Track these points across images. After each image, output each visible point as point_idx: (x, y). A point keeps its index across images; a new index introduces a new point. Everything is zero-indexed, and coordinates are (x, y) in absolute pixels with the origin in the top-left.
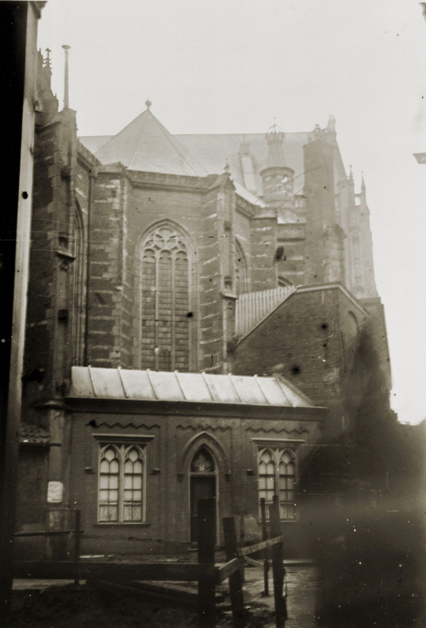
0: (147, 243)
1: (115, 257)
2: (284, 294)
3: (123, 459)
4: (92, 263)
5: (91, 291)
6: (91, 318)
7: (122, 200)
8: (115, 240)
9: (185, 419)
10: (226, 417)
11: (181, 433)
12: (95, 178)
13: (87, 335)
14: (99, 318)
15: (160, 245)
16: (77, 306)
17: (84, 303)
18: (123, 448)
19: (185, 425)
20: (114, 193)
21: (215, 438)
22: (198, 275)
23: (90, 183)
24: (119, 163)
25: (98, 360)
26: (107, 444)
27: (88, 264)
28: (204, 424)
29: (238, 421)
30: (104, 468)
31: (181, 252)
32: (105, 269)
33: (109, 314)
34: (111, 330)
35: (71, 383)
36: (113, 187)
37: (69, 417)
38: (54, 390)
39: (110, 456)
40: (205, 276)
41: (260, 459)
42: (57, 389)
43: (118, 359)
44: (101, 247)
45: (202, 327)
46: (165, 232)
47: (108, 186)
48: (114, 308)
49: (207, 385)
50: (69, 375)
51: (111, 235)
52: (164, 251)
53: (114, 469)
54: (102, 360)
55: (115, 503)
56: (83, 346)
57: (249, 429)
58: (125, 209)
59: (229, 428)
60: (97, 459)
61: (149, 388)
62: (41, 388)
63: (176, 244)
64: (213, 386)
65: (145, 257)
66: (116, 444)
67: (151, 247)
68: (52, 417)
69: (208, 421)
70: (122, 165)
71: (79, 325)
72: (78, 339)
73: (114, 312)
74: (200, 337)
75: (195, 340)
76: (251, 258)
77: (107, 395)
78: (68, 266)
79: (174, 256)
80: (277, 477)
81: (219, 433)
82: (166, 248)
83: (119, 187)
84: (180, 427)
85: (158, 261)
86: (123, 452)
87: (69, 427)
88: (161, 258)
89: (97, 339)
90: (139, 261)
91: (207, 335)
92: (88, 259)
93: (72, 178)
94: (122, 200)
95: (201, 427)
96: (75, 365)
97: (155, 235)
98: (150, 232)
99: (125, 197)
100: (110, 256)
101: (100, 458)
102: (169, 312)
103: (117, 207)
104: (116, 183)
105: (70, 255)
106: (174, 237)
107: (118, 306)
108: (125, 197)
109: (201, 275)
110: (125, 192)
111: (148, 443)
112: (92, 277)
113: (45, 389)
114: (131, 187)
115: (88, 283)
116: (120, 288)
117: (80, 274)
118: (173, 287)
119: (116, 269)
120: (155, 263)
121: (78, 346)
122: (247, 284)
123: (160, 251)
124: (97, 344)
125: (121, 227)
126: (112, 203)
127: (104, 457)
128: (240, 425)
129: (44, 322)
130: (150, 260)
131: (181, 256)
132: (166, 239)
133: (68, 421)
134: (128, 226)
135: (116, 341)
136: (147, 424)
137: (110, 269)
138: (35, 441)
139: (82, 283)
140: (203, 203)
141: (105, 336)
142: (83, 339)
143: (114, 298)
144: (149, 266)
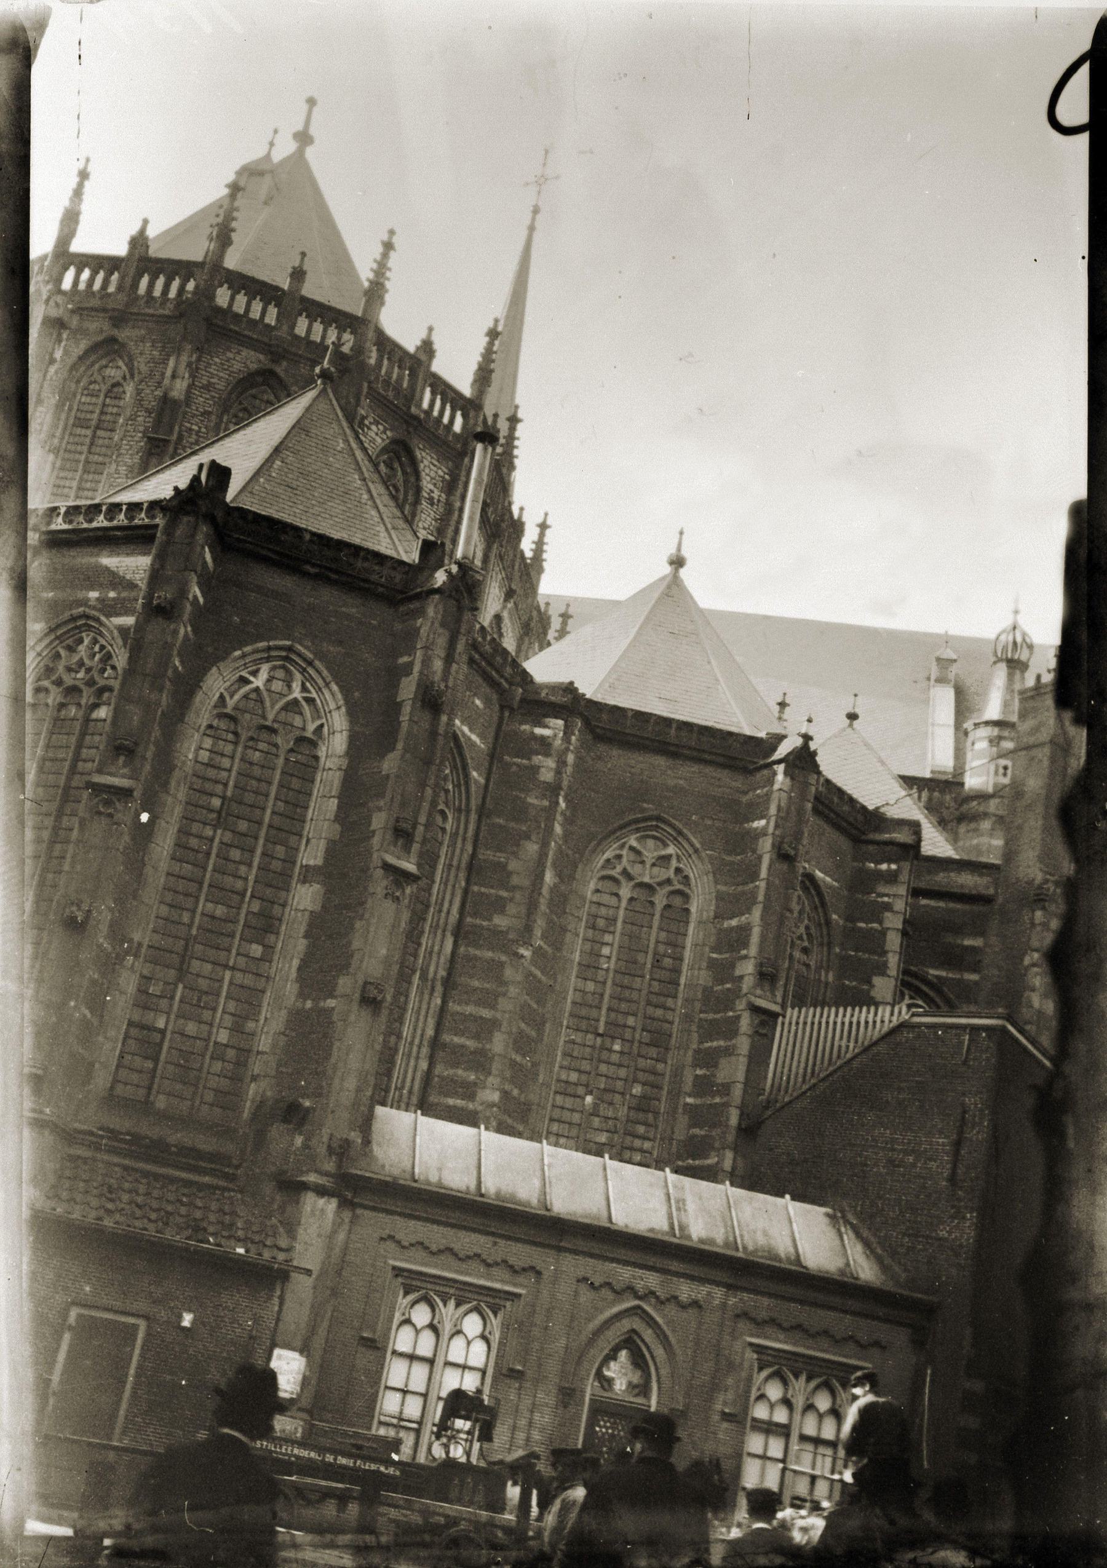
0: (608, 861)
1: (526, 883)
2: (882, 1021)
3: (447, 1328)
4: (476, 888)
5: (462, 949)
6: (453, 1007)
7: (562, 763)
8: (532, 848)
9: (600, 1265)
10: (692, 1278)
11: (586, 1296)
12: (512, 710)
13: (435, 1043)
14: (469, 1009)
15: (635, 870)
16: (424, 977)
17: (442, 973)
18: (452, 1304)
20: (544, 745)
21: (659, 1320)
22: (707, 949)
23: (501, 719)
24: (572, 683)
25: (451, 1101)
26: (417, 1289)
27: (466, 892)
28: (639, 1286)
29: (718, 1293)
30: (403, 1340)
31: (679, 892)
32: (499, 906)
33: (493, 1007)
35: (367, 1142)
36: (546, 732)
37: (347, 1215)
38: (322, 1150)
39: (421, 1315)
40: (720, 953)
41: (759, 1389)
42: (330, 1149)
43: (493, 1105)
44: (501, 857)
45: (695, 1065)
46: (650, 843)
47: (538, 731)
48: (504, 995)
49: (668, 1195)
50: (366, 1124)
51: (528, 837)
52: (641, 885)
53: (426, 1345)
55: (414, 1426)
56: (424, 1065)
57: (743, 1315)
58: (565, 784)
59: (695, 1304)
60: (390, 1319)
61: (537, 1183)
62: (299, 1141)
63: (671, 873)
64: (681, 1204)
65: (597, 891)
66: (438, 1293)
67: (616, 872)
68: (308, 1208)
69: (651, 1280)
70: (576, 689)
71: (422, 1018)
72: (415, 1049)
73: (504, 1004)
74: (688, 1086)
75: (675, 1094)
76: (845, 927)
77: (440, 1185)
79: (660, 900)
80: (794, 1437)
81: (671, 1310)
82: (647, 879)
83: (561, 734)
85: (624, 904)
86: (448, 1312)
87: (341, 1236)
88: (631, 899)
89: (458, 1056)
90: (583, 898)
91: (703, 1086)
92: (468, 881)
93: (445, 707)
94: (562, 763)
95: (631, 1289)
96: (383, 1104)
97: (627, 846)
98: (618, 839)
99: (570, 758)
100: (515, 880)
101: (398, 1317)
102: (631, 1021)
103: (547, 775)
104: (552, 729)
105: (411, 867)
106: (668, 858)
107: (513, 991)
108: (570, 758)
109: (714, 949)
110: (572, 748)
111: (508, 1304)
112: (469, 919)
113: (306, 1146)
114: (590, 737)
115: (458, 932)
116: (526, 953)
118: (649, 966)
120: (618, 908)
121: (412, 1063)
122: (827, 984)
123: (632, 883)
124: (456, 1065)
125: (551, 819)
126: (535, 769)
127: (407, 1316)
128: (724, 1305)
129: (331, 1003)
130: (606, 899)
131: (677, 901)
132: (650, 855)
133: (340, 1224)
134: (569, 821)
135: (496, 1067)
136: (512, 1260)
137: (511, 909)
138: (260, 1254)
139: (444, 931)
140: (746, 793)
142: (425, 1050)
143: (508, 972)
144: (603, 911)
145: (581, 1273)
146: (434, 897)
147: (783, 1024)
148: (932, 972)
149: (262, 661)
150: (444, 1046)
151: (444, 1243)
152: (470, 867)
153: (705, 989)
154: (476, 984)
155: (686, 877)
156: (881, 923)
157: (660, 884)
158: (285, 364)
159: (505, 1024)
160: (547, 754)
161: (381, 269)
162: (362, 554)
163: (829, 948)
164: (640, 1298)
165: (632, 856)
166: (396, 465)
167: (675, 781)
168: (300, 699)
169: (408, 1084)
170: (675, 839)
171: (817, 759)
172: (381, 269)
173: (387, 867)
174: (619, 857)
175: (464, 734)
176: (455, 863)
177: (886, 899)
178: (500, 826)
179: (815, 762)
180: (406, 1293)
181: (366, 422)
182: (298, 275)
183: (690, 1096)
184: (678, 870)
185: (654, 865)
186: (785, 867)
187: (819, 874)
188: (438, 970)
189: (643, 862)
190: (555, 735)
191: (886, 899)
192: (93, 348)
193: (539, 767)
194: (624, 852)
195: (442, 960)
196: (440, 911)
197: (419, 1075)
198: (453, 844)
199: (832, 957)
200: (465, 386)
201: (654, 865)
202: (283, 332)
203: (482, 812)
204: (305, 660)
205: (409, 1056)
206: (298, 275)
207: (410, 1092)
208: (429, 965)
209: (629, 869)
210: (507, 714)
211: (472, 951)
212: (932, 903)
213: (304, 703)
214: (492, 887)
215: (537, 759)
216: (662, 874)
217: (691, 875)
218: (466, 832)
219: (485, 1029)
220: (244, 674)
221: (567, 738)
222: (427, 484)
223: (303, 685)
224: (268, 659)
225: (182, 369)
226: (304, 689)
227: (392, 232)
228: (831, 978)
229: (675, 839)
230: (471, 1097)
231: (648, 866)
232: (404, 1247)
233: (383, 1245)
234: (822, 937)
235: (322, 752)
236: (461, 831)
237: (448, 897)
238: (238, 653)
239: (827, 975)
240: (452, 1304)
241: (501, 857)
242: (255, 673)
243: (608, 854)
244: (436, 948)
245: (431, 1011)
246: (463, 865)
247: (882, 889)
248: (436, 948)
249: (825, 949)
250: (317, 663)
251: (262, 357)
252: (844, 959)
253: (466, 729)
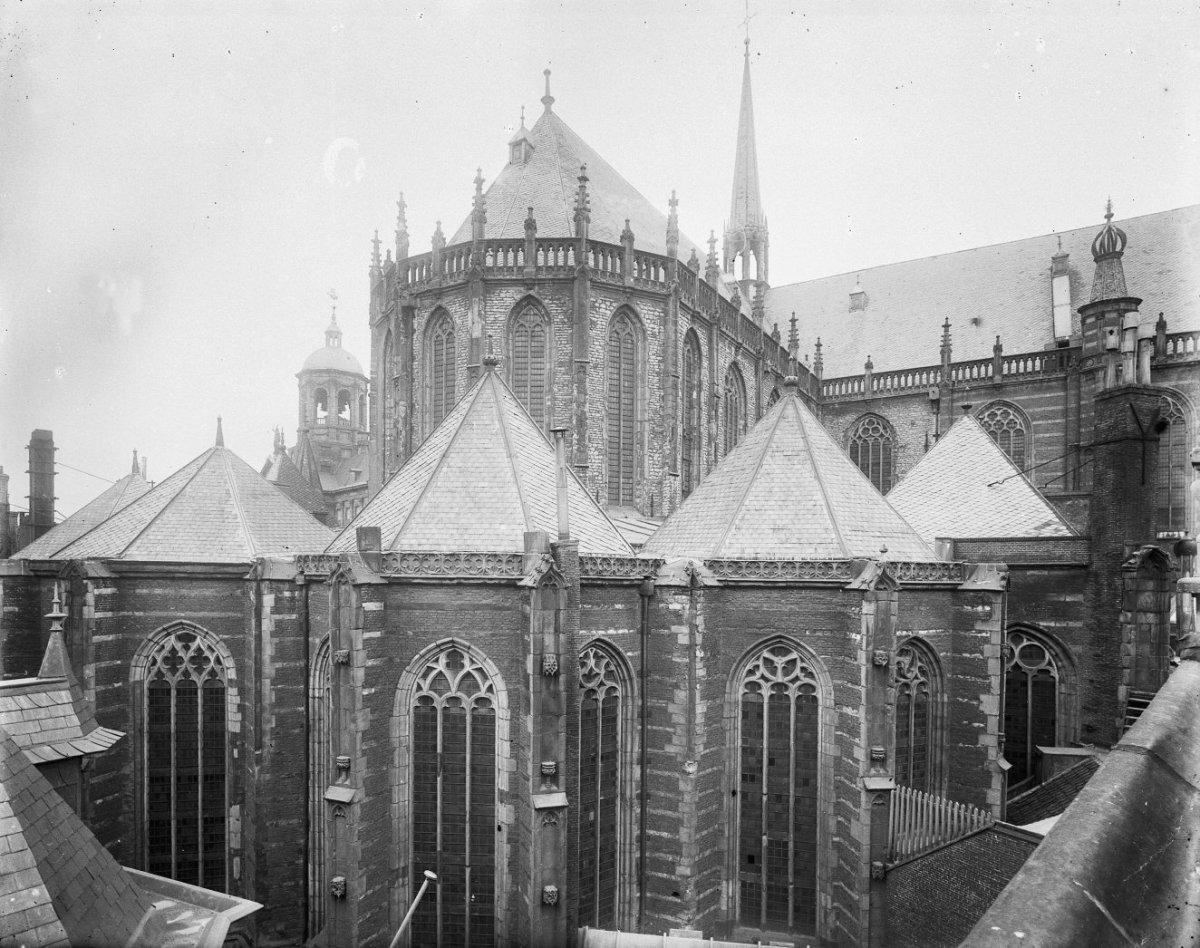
1: (682, 720)
5: (648, 771)
7: (693, 627)
8: (681, 695)
13: (642, 839)
23: (643, 602)
25: (660, 875)
33: (675, 809)
51: (677, 686)
72: (628, 847)
73: (682, 807)
78: (557, 818)
85: (766, 700)
92: (642, 725)
94: (693, 627)
97: (762, 658)
99: (700, 621)
106: (794, 661)
107: (687, 798)
117: (629, 750)
119: (684, 740)
122: (943, 703)
123: (770, 684)
124: (658, 850)
137: (675, 740)
139: (632, 764)
141: (668, 841)
143: (682, 786)
146: (619, 744)
147: (895, 796)
148: (1042, 624)
149: (438, 653)
150: (649, 837)
152: (642, 715)
153: (836, 758)
154: (662, 794)
156: (982, 653)
158: (536, 288)
159: (685, 820)
160: (680, 623)
163: (942, 676)
166: (627, 320)
167: (789, 607)
169: (627, 871)
175: (610, 636)
176: (629, 715)
177: (984, 634)
178: (659, 682)
181: (597, 305)
182: (530, 225)
183: (836, 836)
187: (922, 633)
188: (632, 791)
190: (683, 608)
191: (984, 634)
192: (433, 314)
193: (677, 634)
194: (760, 662)
196: (626, 752)
197: (634, 864)
198: (625, 705)
199: (945, 682)
202: (530, 269)
203: (642, 674)
204: (465, 646)
205: (624, 852)
206: (530, 225)
207: (630, 875)
210: (646, 599)
211: (656, 772)
212: (1036, 572)
214: (661, 725)
215: (674, 629)
217: (814, 671)
218: (633, 693)
219: (674, 825)
221: (693, 607)
222: (649, 325)
223: (471, 659)
224: (442, 651)
225: (477, 318)
226: (472, 662)
228: (946, 699)
230: (673, 872)
234: (934, 670)
235: (494, 705)
237: (629, 739)
238: (417, 657)
239: (942, 696)
241: (662, 703)
242: (437, 661)
244: (628, 776)
245: (634, 821)
247: (979, 626)
248: (628, 776)
249: (938, 677)
250: (473, 647)
251: (522, 289)
252: (954, 681)
253: (611, 631)
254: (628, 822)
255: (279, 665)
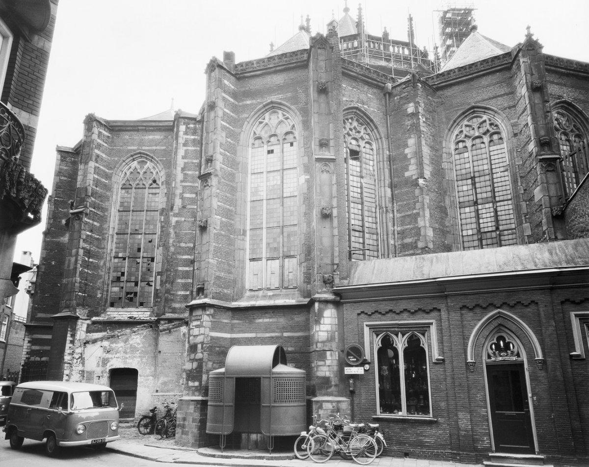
19: (470, 305)
34: (416, 222)
54: (411, 252)
63: (488, 127)
82: (477, 134)
84: (464, 307)
106: (485, 121)
145: (461, 305)
151: (388, 308)
155: (496, 126)
157: (485, 134)
161: (360, 17)
162: (288, 55)
164: (498, 308)
165: (468, 129)
168: (283, 120)
170: (485, 112)
171: (539, 41)
172: (360, 17)
173: (318, 160)
174: (461, 132)
179: (539, 44)
180: (377, 336)
184: (491, 124)
185: (479, 128)
186: (538, 95)
189: (473, 129)
195: (387, 199)
200: (406, 39)
201: (479, 128)
208: (382, 203)
209: (468, 134)
213: (285, 120)
216: (482, 130)
220: (260, 120)
223: (282, 114)
226: (284, 115)
227: (360, 4)
229: (485, 112)
231: (476, 129)
232: (370, 315)
233: (360, 317)
236: (381, 147)
240: (400, 335)
242: (264, 119)
243: (456, 132)
246: (385, 159)
254: (384, 221)
255: (186, 161)
